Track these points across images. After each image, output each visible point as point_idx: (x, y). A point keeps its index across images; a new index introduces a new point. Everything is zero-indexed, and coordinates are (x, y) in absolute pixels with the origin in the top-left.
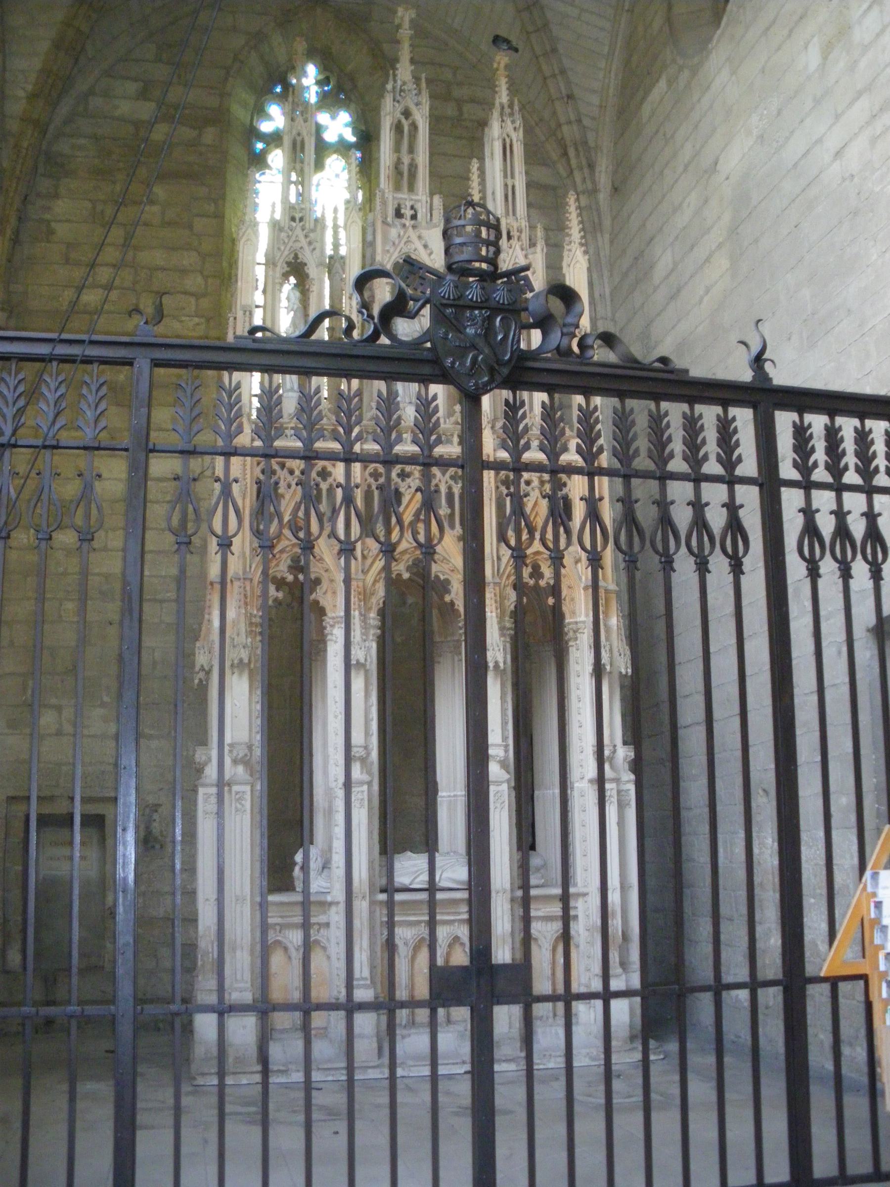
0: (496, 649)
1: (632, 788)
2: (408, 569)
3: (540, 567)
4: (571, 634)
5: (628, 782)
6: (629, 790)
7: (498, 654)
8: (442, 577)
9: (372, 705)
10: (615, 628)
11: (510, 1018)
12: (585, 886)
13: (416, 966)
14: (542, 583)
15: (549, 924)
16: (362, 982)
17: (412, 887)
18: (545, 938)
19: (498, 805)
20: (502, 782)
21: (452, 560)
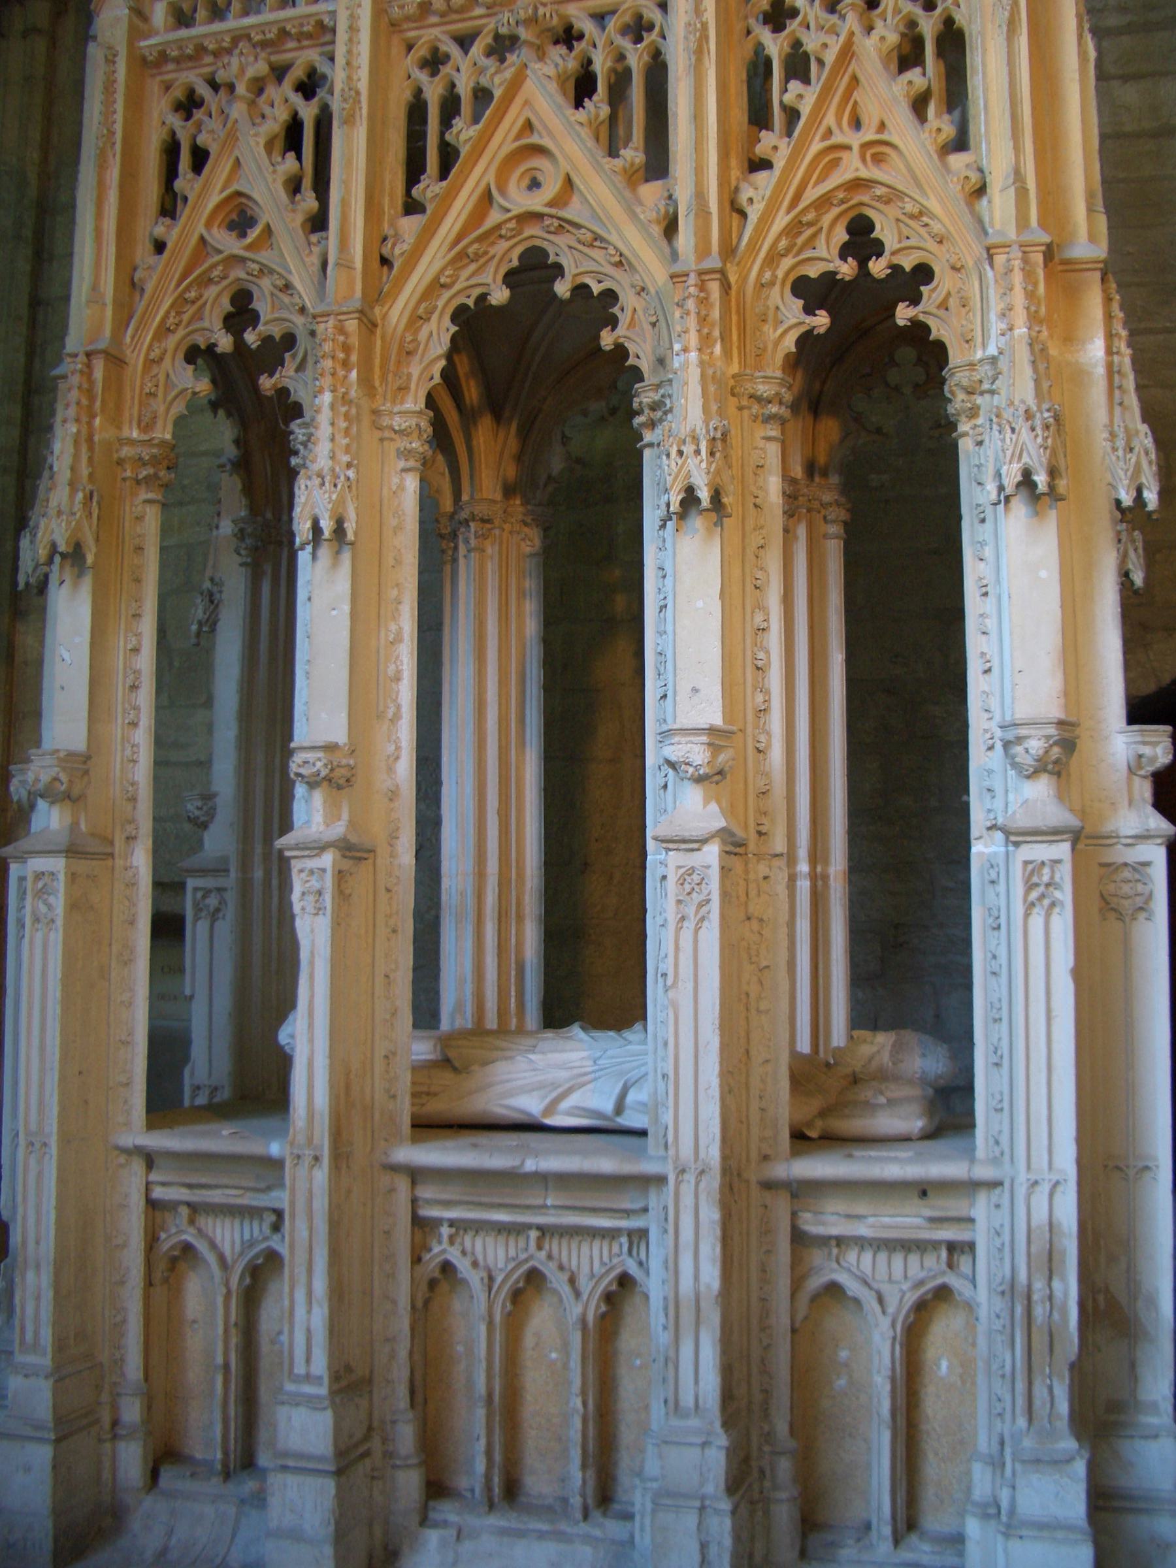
0: (688, 449)
1: (1158, 856)
2: (511, 278)
3: (871, 227)
4: (961, 396)
5: (1144, 837)
6: (1147, 864)
7: (692, 463)
8: (596, 289)
9: (398, 639)
10: (1100, 370)
11: (704, 1546)
12: (996, 1161)
13: (529, 1340)
14: (878, 268)
15: (898, 1260)
16: (308, 1389)
17: (548, 1121)
18: (881, 1300)
19: (690, 911)
20: (704, 841)
21: (614, 238)
